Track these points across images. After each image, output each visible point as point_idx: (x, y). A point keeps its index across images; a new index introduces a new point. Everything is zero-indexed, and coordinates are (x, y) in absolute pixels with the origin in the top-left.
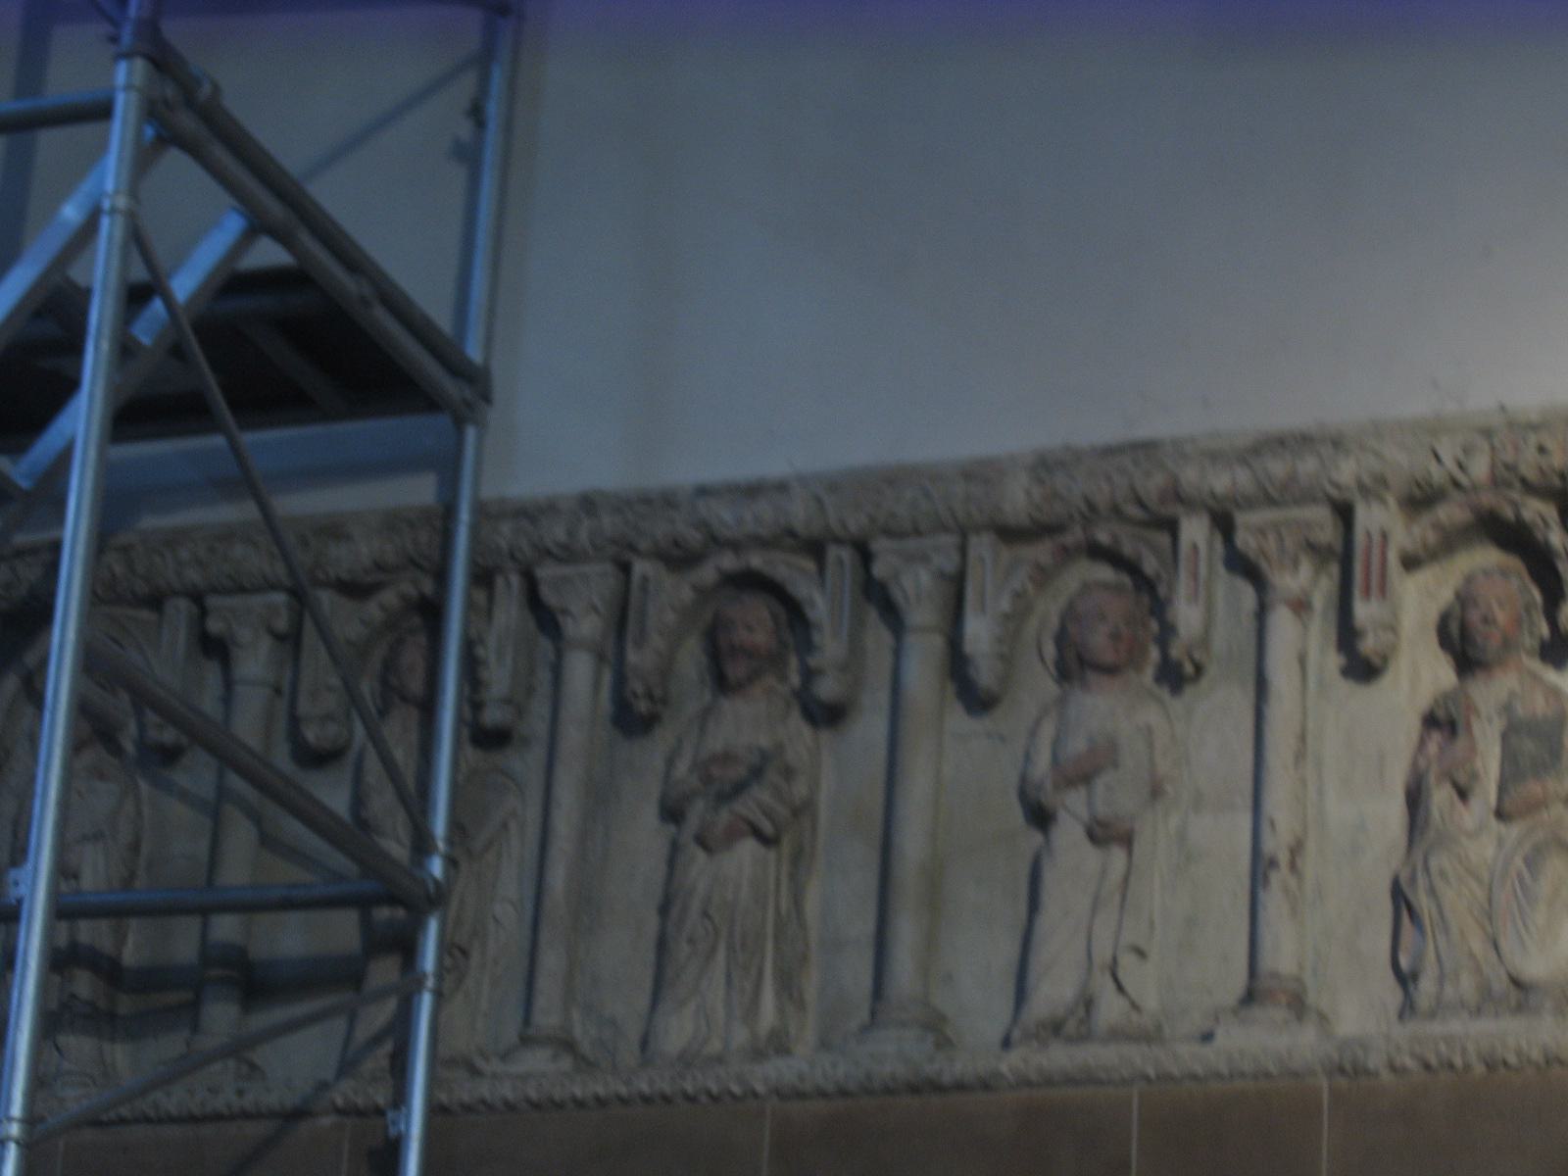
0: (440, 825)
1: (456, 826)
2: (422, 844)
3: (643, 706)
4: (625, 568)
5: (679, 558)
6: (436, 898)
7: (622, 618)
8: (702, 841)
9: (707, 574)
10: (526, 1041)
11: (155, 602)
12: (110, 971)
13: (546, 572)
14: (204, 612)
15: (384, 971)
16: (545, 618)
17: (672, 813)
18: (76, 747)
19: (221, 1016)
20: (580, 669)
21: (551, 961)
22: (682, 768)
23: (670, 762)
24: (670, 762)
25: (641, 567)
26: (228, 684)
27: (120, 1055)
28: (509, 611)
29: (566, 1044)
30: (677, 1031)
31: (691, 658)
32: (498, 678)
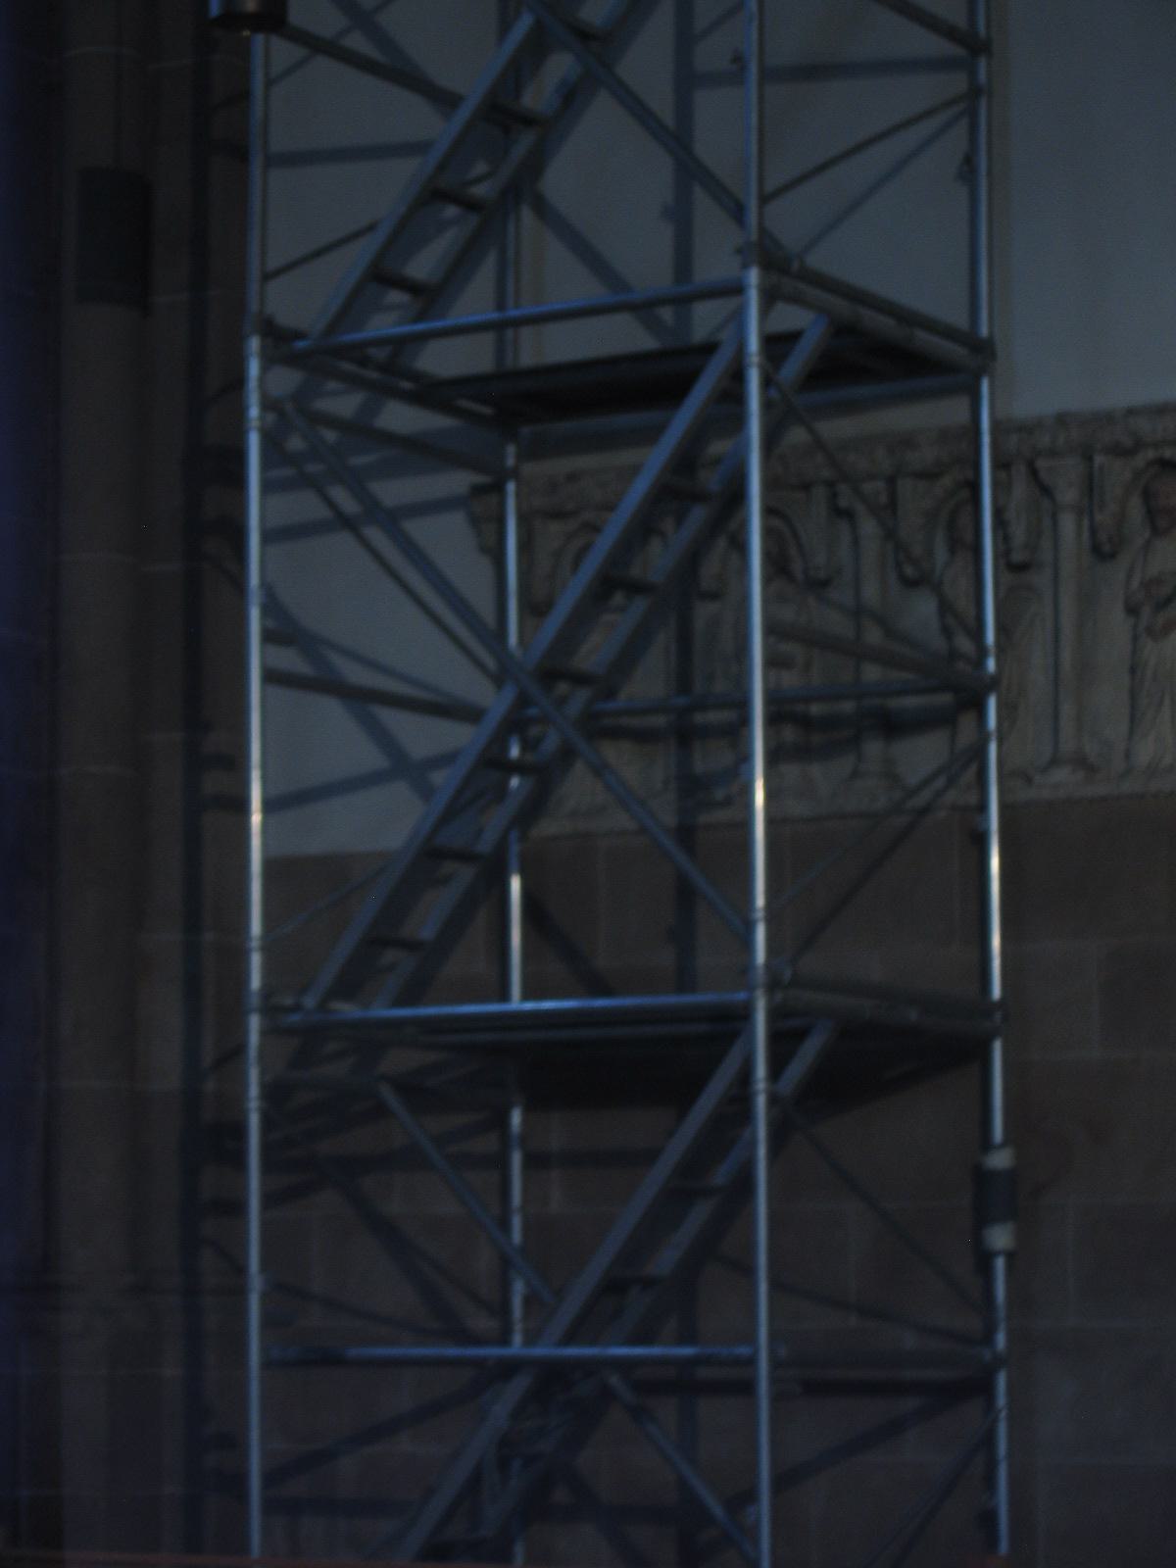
0: (990, 636)
1: (1001, 628)
2: (982, 652)
3: (1107, 548)
4: (1090, 459)
5: (1119, 451)
6: (994, 683)
7: (1091, 486)
8: (1150, 631)
9: (1140, 460)
10: (1055, 762)
11: (806, 487)
12: (805, 723)
13: (1042, 464)
14: (835, 495)
15: (967, 723)
16: (1046, 491)
17: (1132, 610)
18: (767, 581)
19: (873, 748)
20: (1068, 523)
21: (1067, 709)
22: (1135, 584)
23: (1129, 576)
24: (1129, 576)
25: (1098, 459)
26: (856, 542)
27: (816, 770)
28: (1021, 490)
29: (1081, 762)
30: (1145, 752)
31: (1136, 509)
32: (1019, 533)
